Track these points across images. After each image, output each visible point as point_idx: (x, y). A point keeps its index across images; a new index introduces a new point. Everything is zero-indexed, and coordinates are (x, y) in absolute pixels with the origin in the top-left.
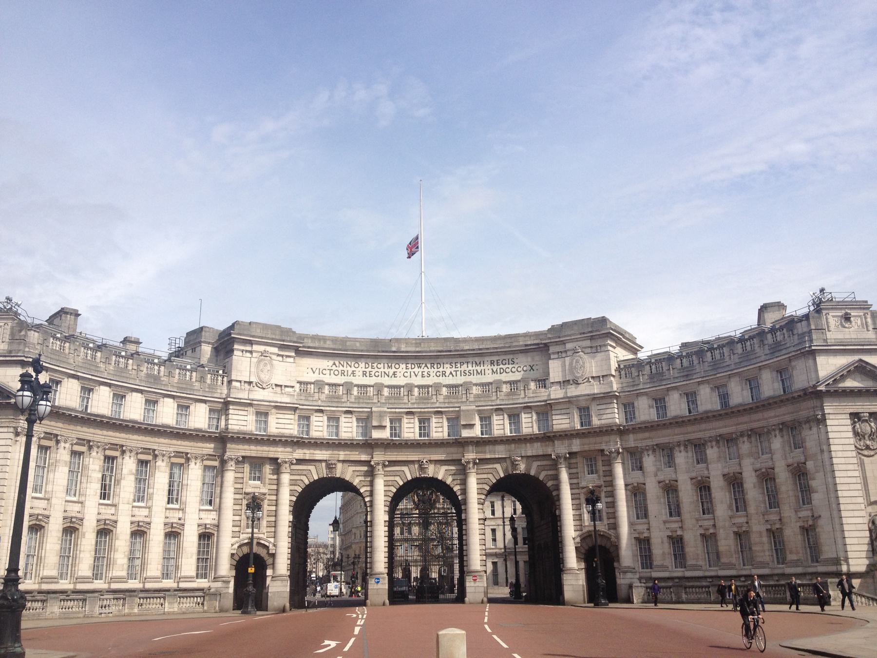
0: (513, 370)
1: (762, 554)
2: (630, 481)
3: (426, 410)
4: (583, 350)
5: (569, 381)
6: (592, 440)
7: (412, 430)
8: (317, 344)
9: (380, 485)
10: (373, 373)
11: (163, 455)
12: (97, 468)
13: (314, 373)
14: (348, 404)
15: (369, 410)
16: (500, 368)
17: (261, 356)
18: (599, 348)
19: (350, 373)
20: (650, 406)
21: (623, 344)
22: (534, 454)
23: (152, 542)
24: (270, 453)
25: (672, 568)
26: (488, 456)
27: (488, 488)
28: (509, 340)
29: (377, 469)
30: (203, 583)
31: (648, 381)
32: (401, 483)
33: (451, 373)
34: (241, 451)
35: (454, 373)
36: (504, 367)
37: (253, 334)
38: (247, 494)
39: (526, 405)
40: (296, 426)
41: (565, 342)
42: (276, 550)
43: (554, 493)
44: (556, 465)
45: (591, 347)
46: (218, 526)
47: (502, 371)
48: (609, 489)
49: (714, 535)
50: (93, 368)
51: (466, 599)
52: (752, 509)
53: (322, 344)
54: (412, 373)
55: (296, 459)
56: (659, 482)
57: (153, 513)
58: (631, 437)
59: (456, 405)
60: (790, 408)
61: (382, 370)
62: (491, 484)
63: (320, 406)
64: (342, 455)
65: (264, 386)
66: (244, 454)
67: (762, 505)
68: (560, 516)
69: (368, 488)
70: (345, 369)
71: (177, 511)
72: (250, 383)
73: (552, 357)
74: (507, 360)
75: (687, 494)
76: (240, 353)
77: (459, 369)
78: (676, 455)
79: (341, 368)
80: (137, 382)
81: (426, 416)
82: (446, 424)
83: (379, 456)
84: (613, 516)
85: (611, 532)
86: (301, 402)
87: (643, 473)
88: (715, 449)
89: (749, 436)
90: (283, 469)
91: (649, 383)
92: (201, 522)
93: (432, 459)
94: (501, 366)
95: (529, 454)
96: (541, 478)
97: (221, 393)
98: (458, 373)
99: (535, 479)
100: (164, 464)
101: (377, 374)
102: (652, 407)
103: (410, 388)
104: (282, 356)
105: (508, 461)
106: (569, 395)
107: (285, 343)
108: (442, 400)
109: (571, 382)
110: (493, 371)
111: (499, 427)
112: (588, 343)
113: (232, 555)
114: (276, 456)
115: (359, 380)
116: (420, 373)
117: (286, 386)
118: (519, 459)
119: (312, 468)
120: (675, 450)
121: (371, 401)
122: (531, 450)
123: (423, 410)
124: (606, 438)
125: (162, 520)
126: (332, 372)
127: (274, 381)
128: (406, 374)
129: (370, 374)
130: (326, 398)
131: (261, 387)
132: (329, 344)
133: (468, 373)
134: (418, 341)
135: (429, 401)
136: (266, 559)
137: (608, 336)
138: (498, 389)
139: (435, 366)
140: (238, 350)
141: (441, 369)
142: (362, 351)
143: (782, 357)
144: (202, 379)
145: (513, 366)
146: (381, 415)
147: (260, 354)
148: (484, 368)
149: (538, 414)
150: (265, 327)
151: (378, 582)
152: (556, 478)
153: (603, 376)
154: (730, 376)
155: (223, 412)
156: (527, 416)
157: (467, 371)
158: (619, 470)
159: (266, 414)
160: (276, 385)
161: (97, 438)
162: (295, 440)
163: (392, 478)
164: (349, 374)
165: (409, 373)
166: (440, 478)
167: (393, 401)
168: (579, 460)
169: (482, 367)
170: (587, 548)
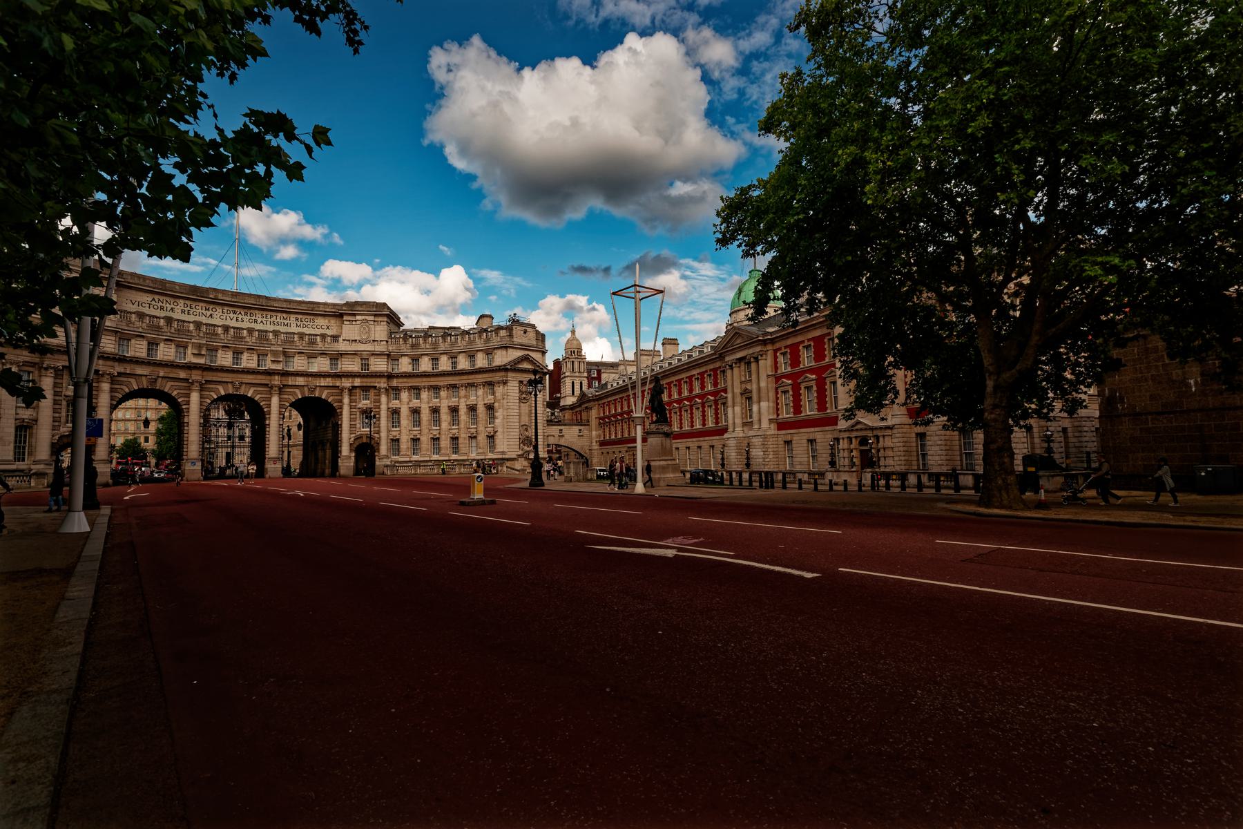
2: (390, 406)
6: (369, 380)
8: (136, 281)
9: (195, 397)
14: (169, 334)
19: (169, 309)
26: (290, 383)
28: (312, 306)
30: (22, 466)
46: (36, 421)
49: (438, 439)
52: (462, 425)
58: (395, 380)
60: (491, 375)
68: (341, 425)
69: (186, 399)
70: (164, 305)
75: (425, 415)
83: (196, 376)
89: (466, 387)
92: (18, 417)
96: (329, 400)
99: (325, 401)
112: (372, 318)
113: (53, 443)
115: (177, 315)
119: (133, 381)
122: (323, 382)
124: (378, 380)
141: (254, 318)
143: (491, 345)
146: (200, 346)
152: (341, 401)
154: (460, 352)
158: (384, 399)
163: (208, 393)
164: (169, 309)
166: (249, 395)
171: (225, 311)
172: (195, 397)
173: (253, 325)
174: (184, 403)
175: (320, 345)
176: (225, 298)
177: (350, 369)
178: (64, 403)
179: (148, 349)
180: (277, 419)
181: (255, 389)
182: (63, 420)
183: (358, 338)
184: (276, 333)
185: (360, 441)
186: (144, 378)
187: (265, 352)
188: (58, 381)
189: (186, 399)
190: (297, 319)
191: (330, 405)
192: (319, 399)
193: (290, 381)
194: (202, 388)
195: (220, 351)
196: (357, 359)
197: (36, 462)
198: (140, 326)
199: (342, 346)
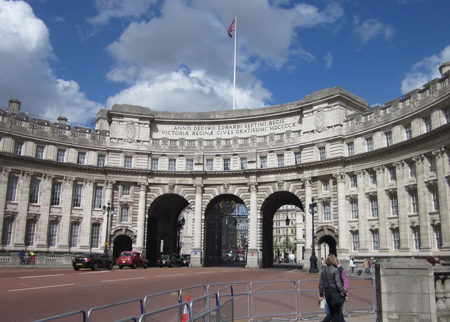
0: (283, 127)
1: (427, 242)
3: (228, 153)
4: (323, 109)
5: (313, 131)
7: (219, 166)
9: (198, 197)
10: (199, 133)
11: (70, 180)
12: (27, 185)
13: (163, 134)
14: (181, 151)
17: (128, 124)
18: (333, 107)
19: (185, 133)
20: (363, 144)
21: (353, 105)
22: (291, 179)
23: (63, 227)
24: (133, 179)
25: (372, 250)
27: (263, 200)
29: (197, 189)
31: (363, 127)
32: (212, 197)
33: (245, 131)
34: (115, 178)
35: (247, 131)
36: (277, 125)
37: (124, 111)
38: (120, 202)
39: (287, 148)
40: (150, 165)
42: (137, 233)
43: (303, 203)
45: (328, 107)
47: (276, 127)
48: (336, 199)
50: (23, 131)
51: (246, 266)
53: (168, 117)
54: (222, 132)
55: (149, 183)
56: (366, 194)
57: (62, 211)
59: (247, 150)
61: (204, 131)
62: (265, 198)
63: (164, 153)
64: (177, 180)
65: (130, 141)
67: (429, 207)
69: (193, 200)
70: (182, 131)
71: (79, 211)
72: (122, 139)
73: (305, 116)
74: (279, 121)
78: (377, 176)
79: (180, 130)
80: (52, 139)
81: (228, 157)
82: (239, 161)
83: (198, 181)
84: (336, 216)
85: (336, 227)
86: (152, 151)
87: (357, 188)
88: (401, 169)
90: (142, 189)
91: (363, 128)
92: (93, 217)
94: (276, 125)
95: (289, 179)
96: (295, 194)
97: (105, 146)
98: (250, 130)
100: (70, 184)
101: (201, 133)
102: (365, 144)
103: (219, 141)
104: (142, 124)
105: (276, 184)
106: (314, 140)
107: (143, 116)
108: (237, 147)
109: (315, 131)
110: (271, 128)
111: (271, 163)
112: (326, 105)
115: (190, 137)
116: (227, 132)
117: (143, 141)
118: (282, 182)
120: (376, 173)
121: (195, 149)
123: (225, 153)
125: (69, 215)
126: (174, 133)
127: (137, 138)
128: (218, 133)
129: (197, 133)
130: (168, 148)
131: (128, 141)
132: (173, 116)
134: (226, 112)
135: (230, 148)
136: (132, 238)
137: (338, 99)
138: (272, 138)
139: (236, 127)
140: (114, 120)
141: (240, 129)
142: (191, 120)
144: (93, 138)
145: (283, 124)
149: (295, 153)
150: (132, 107)
151: (196, 254)
152: (304, 193)
155: (107, 156)
156: (288, 155)
158: (341, 186)
159: (131, 157)
160: (137, 140)
162: (148, 172)
164: (184, 134)
165: (220, 132)
166: (235, 194)
167: (208, 149)
169: (264, 126)
170: (321, 237)
171: (221, 128)
172: (198, 197)
173: (240, 135)
174: (193, 203)
175: (286, 142)
176: (221, 117)
177: (309, 161)
178: (119, 206)
179: (169, 164)
180: (256, 214)
183: (314, 128)
184: (253, 138)
186: (167, 186)
187: (245, 156)
189: (193, 200)
193: (264, 178)
194: (203, 192)
195: (214, 160)
196: (316, 149)
198: (163, 148)
199: (304, 139)
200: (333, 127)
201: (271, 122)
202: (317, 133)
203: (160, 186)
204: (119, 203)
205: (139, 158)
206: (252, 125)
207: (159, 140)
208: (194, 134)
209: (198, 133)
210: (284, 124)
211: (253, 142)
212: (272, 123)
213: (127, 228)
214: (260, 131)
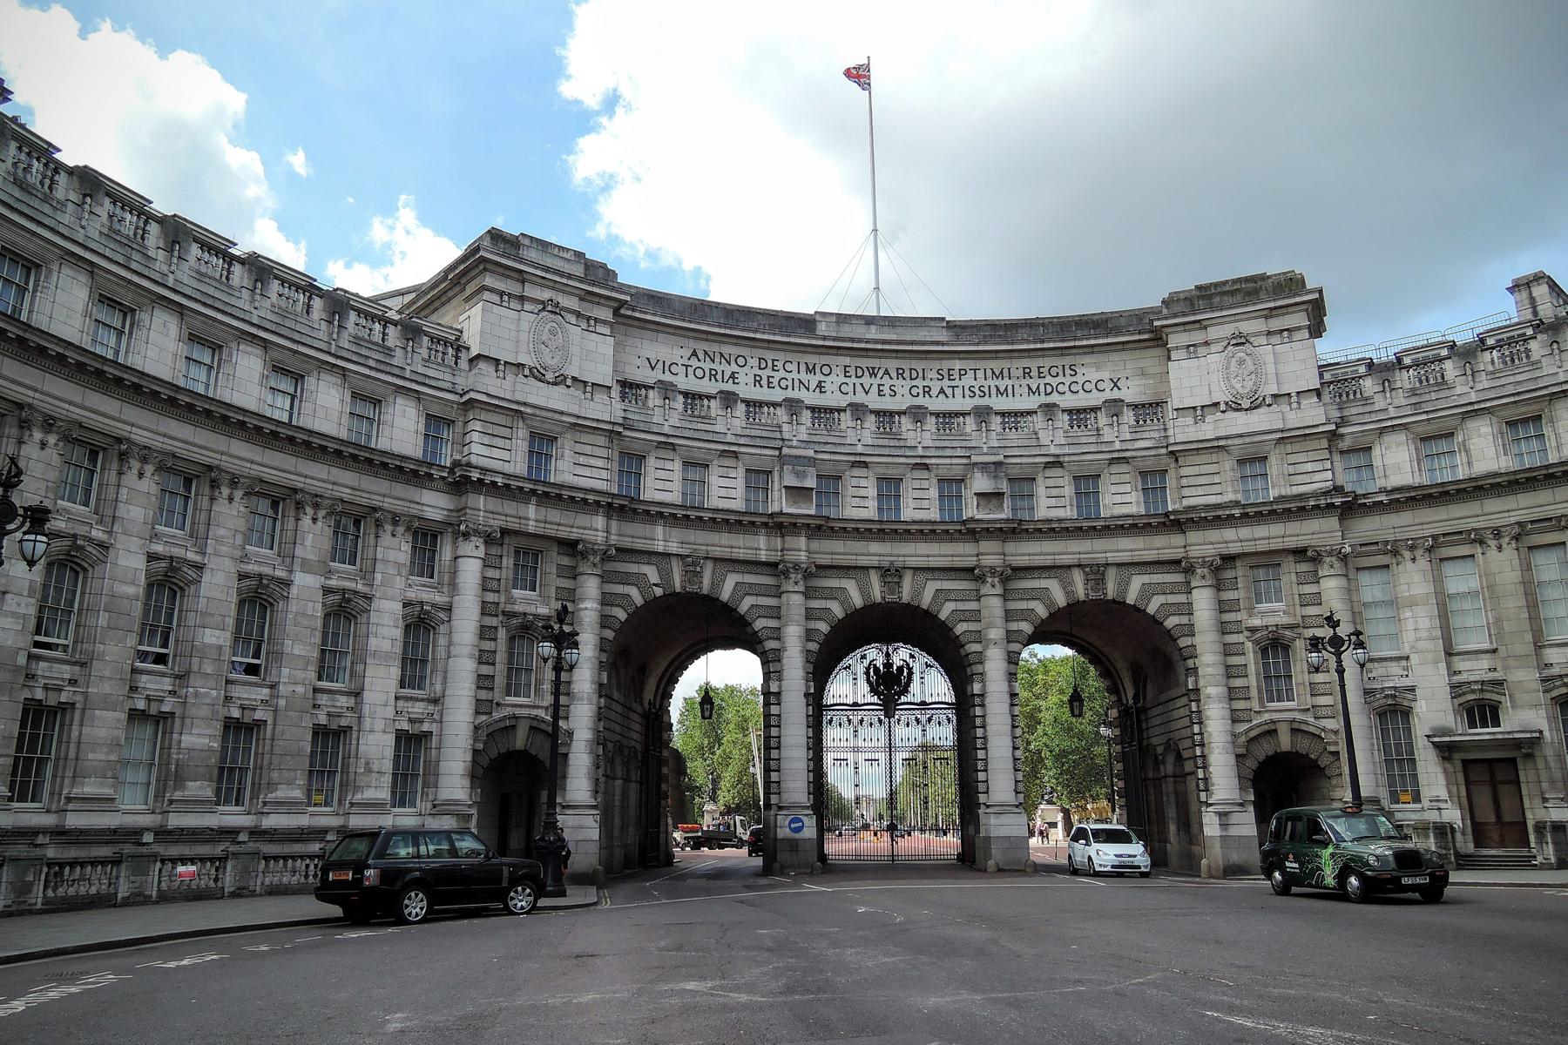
5: (1216, 404)
10: (775, 381)
15: (777, 453)
16: (1045, 384)
24: (560, 528)
33: (942, 391)
34: (496, 516)
35: (949, 391)
36: (1054, 381)
38: (510, 615)
41: (1205, 323)
44: (1188, 583)
47: (1049, 389)
51: (991, 863)
54: (859, 388)
59: (959, 452)
61: (795, 375)
66: (503, 524)
69: (773, 623)
72: (520, 366)
74: (1061, 368)
76: (496, 299)
77: (960, 384)
82: (934, 493)
93: (909, 564)
94: (1049, 379)
96: (1151, 609)
101: (783, 384)
109: (1223, 407)
110: (1030, 388)
112: (1258, 325)
114: (574, 536)
115: (746, 390)
116: (875, 388)
117: (593, 384)
127: (572, 371)
128: (844, 388)
129: (769, 383)
133: (978, 392)
139: (907, 375)
140: (492, 290)
141: (919, 383)
145: (1074, 379)
147: (541, 307)
148: (1010, 383)
152: (1187, 608)
153: (1298, 393)
157: (977, 387)
160: (574, 379)
161: (140, 437)
165: (851, 385)
168: (1240, 572)
170: (1261, 758)
171: (852, 371)
178: (502, 634)
181: (938, 585)
182: (500, 681)
183: (1221, 396)
185: (1265, 749)
187: (957, 472)
188: (490, 573)
189: (773, 623)
190: (1027, 373)
191: (1155, 622)
192: (1118, 605)
197: (438, 809)
198: (668, 417)
200: (1294, 399)
201: (1027, 370)
202: (1231, 414)
203: (646, 558)
204: (501, 618)
205: (579, 448)
206: (963, 372)
207: (647, 387)
208: (759, 382)
209: (771, 380)
210: (1080, 379)
211: (984, 429)
212: (1034, 373)
213: (535, 724)
214: (994, 396)
